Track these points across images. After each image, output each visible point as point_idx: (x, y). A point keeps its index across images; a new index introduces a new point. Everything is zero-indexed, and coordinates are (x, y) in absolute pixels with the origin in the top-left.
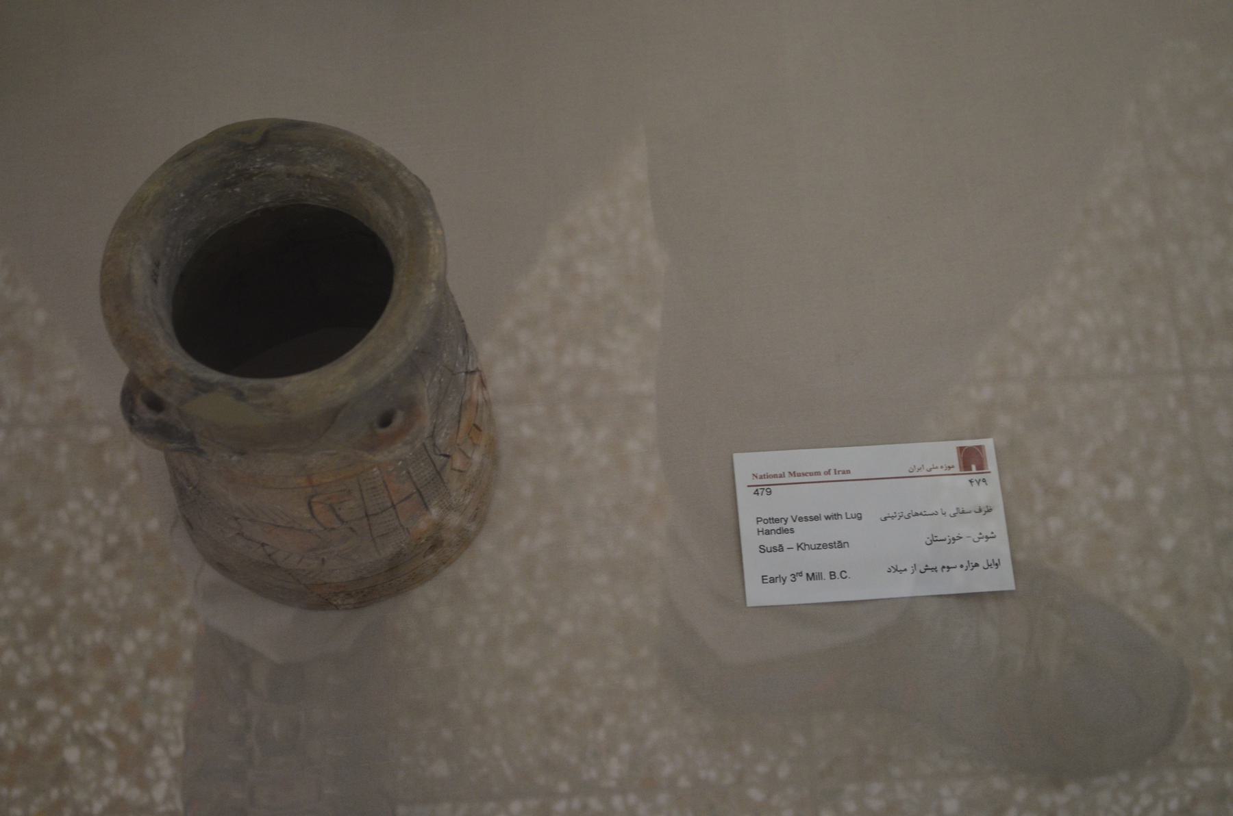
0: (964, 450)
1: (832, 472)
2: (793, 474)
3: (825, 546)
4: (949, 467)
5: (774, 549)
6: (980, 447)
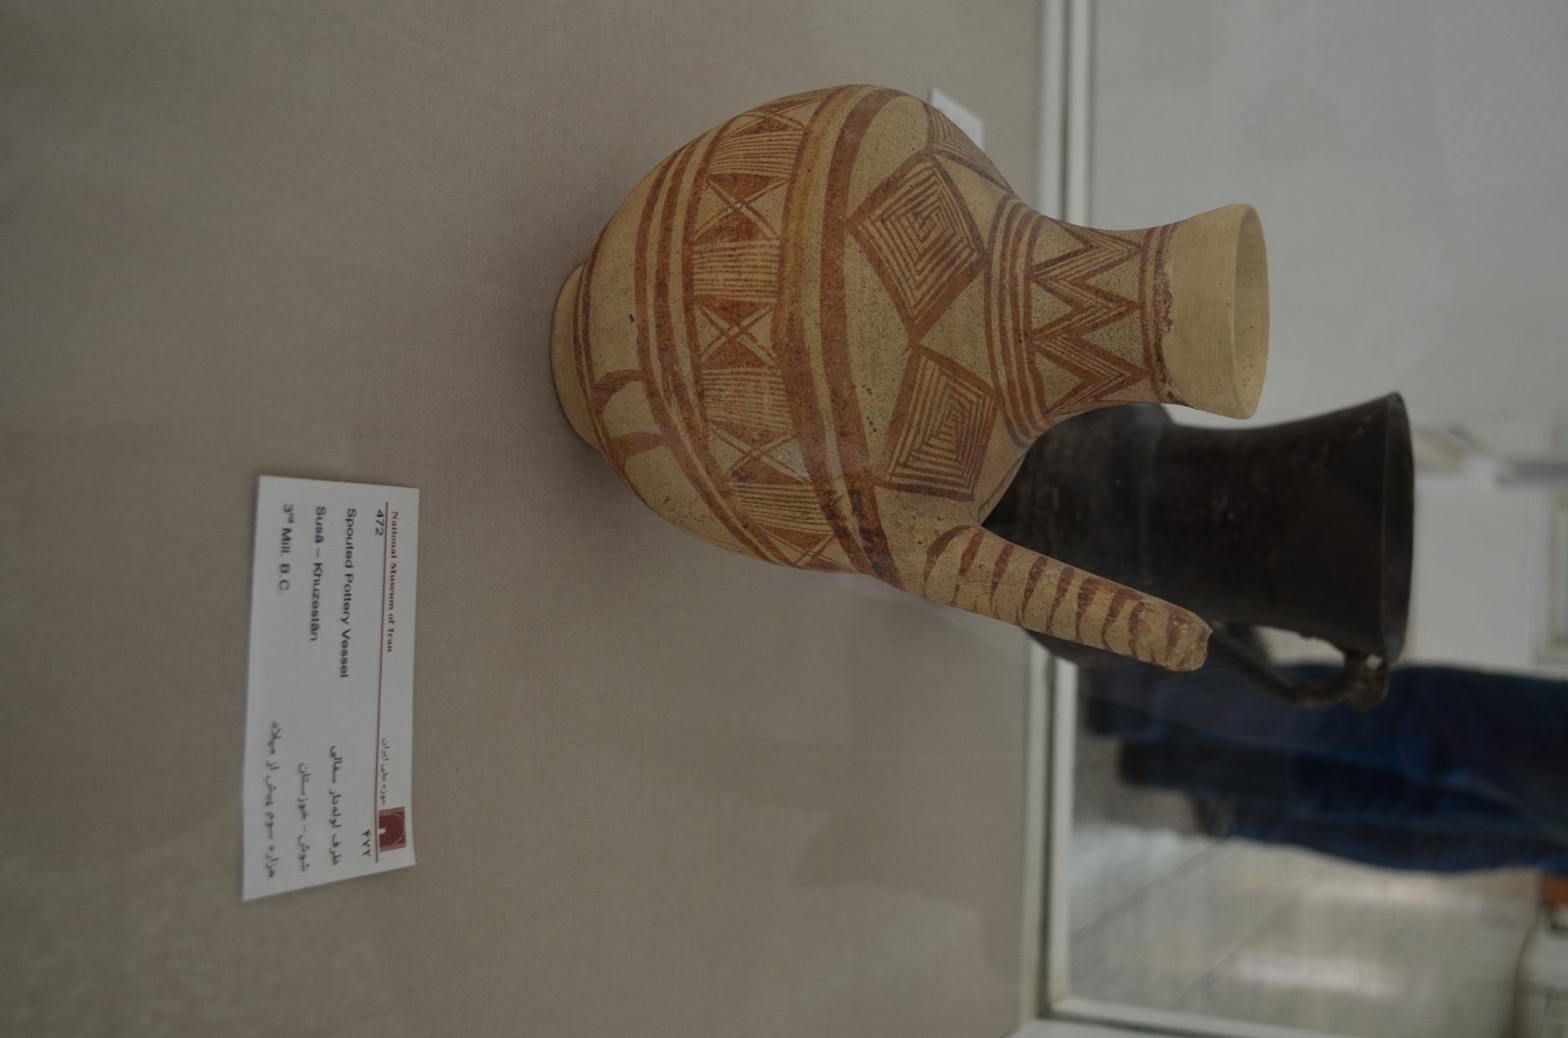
0: (399, 816)
3: (315, 605)
4: (383, 797)
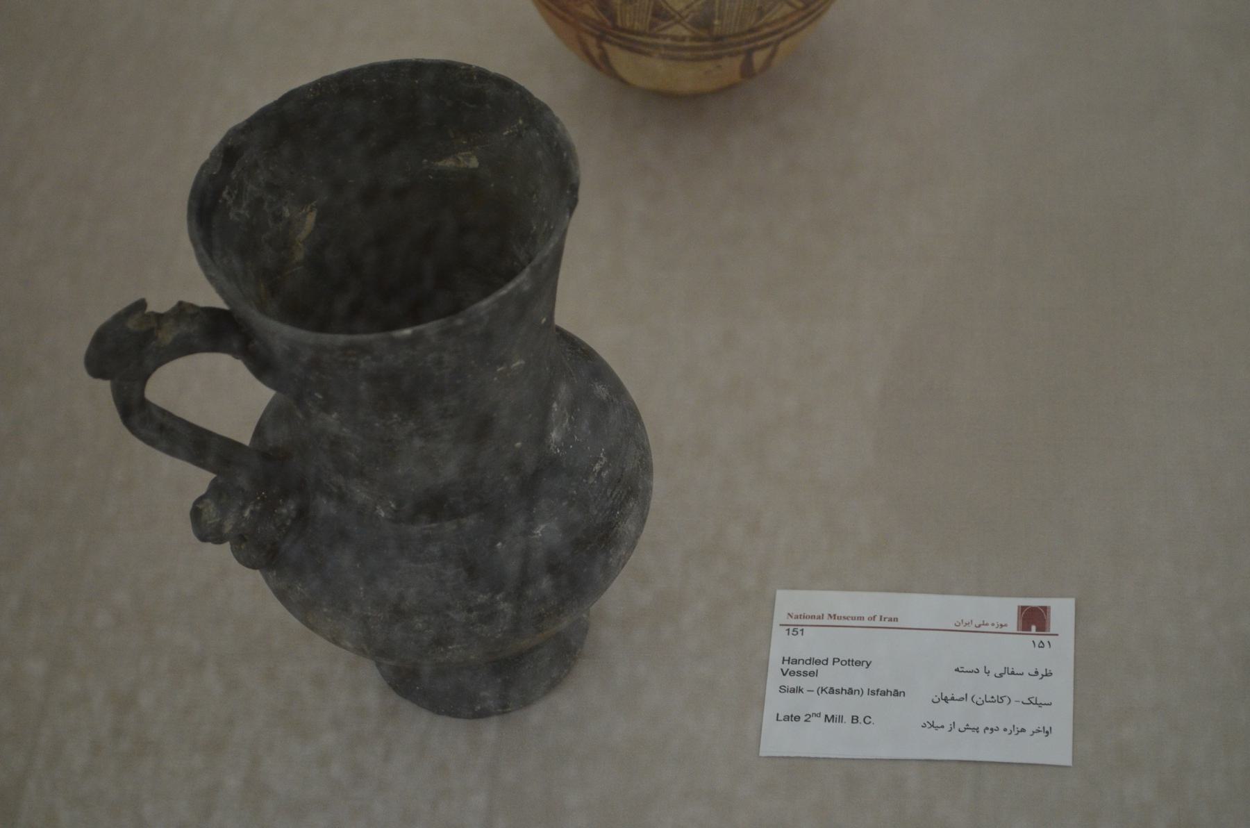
1: (878, 618)
2: (834, 617)
5: (793, 691)
6: (1045, 609)
